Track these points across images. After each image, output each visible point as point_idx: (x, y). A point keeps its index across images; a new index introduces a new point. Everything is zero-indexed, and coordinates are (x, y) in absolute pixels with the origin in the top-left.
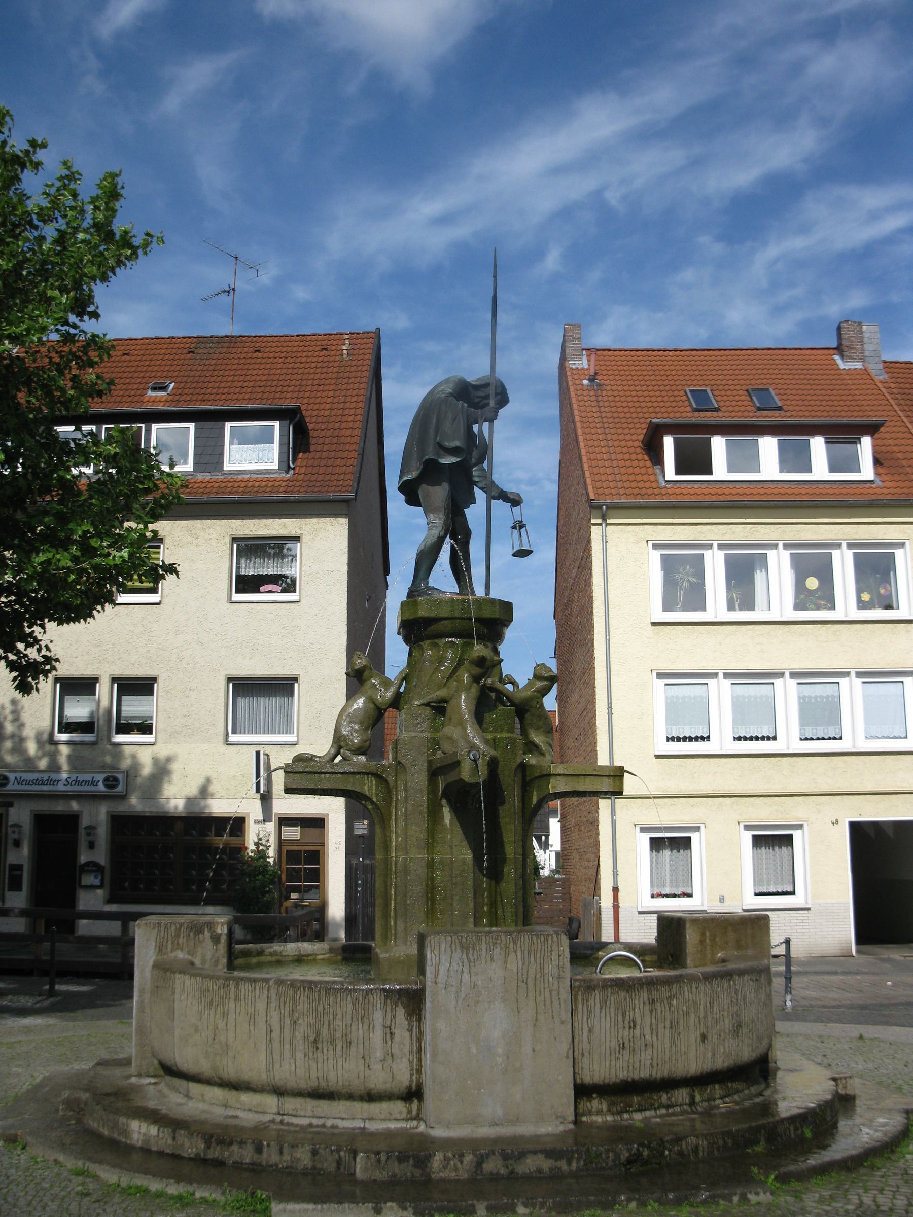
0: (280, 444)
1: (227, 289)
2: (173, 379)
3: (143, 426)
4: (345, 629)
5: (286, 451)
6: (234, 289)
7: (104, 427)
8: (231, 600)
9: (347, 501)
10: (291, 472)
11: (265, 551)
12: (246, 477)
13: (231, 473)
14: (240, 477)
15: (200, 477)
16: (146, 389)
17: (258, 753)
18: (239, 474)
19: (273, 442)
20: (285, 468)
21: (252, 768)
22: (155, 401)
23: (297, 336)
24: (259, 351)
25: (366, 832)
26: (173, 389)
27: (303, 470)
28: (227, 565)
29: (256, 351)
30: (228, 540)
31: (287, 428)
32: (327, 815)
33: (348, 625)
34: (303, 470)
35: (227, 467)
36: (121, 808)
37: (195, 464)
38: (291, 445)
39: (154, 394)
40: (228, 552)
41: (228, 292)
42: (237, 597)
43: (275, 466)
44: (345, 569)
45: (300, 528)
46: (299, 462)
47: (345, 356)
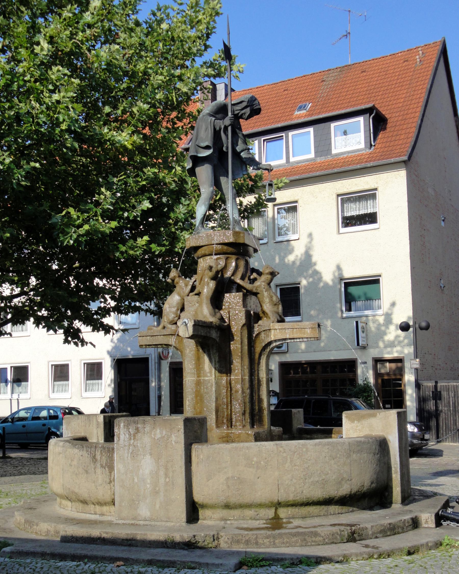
0: (365, 132)
1: (346, 34)
2: (311, 101)
3: (284, 134)
4: (408, 242)
5: (368, 135)
6: (349, 33)
7: (262, 139)
8: (339, 232)
9: (404, 162)
10: (373, 148)
11: (350, 200)
12: (345, 156)
13: (336, 155)
14: (342, 156)
15: (319, 160)
16: (294, 111)
17: (357, 323)
18: (341, 155)
19: (360, 132)
20: (369, 146)
21: (354, 330)
22: (299, 117)
23: (390, 55)
24: (364, 72)
25: (418, 366)
26: (310, 107)
27: (380, 146)
28: (335, 211)
29: (362, 72)
30: (335, 196)
31: (368, 120)
32: (373, 358)
33: (410, 239)
34: (380, 146)
35: (334, 152)
36: (289, 358)
37: (316, 152)
38: (372, 131)
39: (299, 113)
40: (335, 203)
41: (346, 35)
42: (343, 230)
43: (362, 146)
44: (406, 204)
45: (377, 183)
46: (378, 141)
47: (418, 63)
